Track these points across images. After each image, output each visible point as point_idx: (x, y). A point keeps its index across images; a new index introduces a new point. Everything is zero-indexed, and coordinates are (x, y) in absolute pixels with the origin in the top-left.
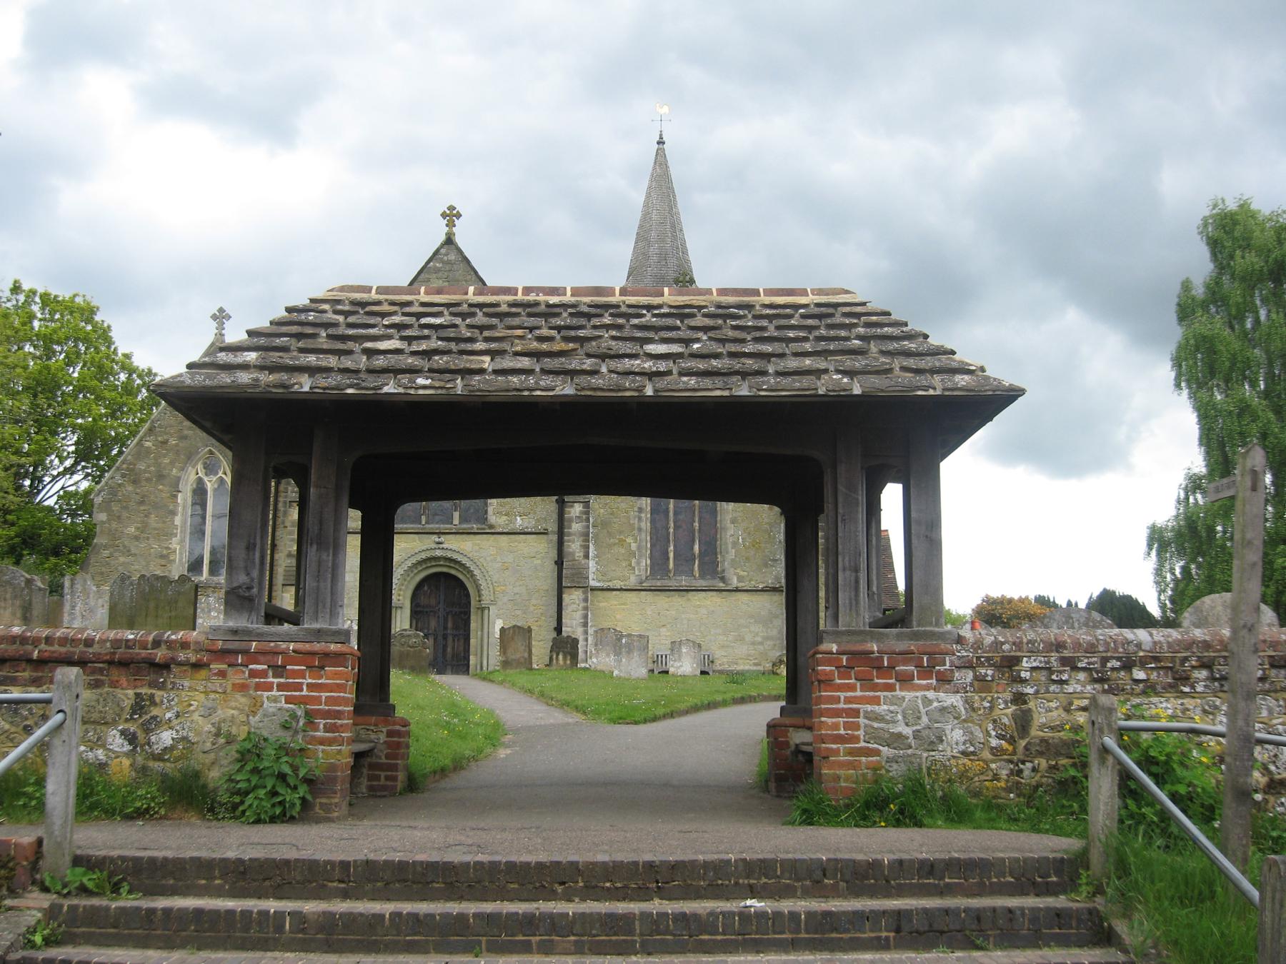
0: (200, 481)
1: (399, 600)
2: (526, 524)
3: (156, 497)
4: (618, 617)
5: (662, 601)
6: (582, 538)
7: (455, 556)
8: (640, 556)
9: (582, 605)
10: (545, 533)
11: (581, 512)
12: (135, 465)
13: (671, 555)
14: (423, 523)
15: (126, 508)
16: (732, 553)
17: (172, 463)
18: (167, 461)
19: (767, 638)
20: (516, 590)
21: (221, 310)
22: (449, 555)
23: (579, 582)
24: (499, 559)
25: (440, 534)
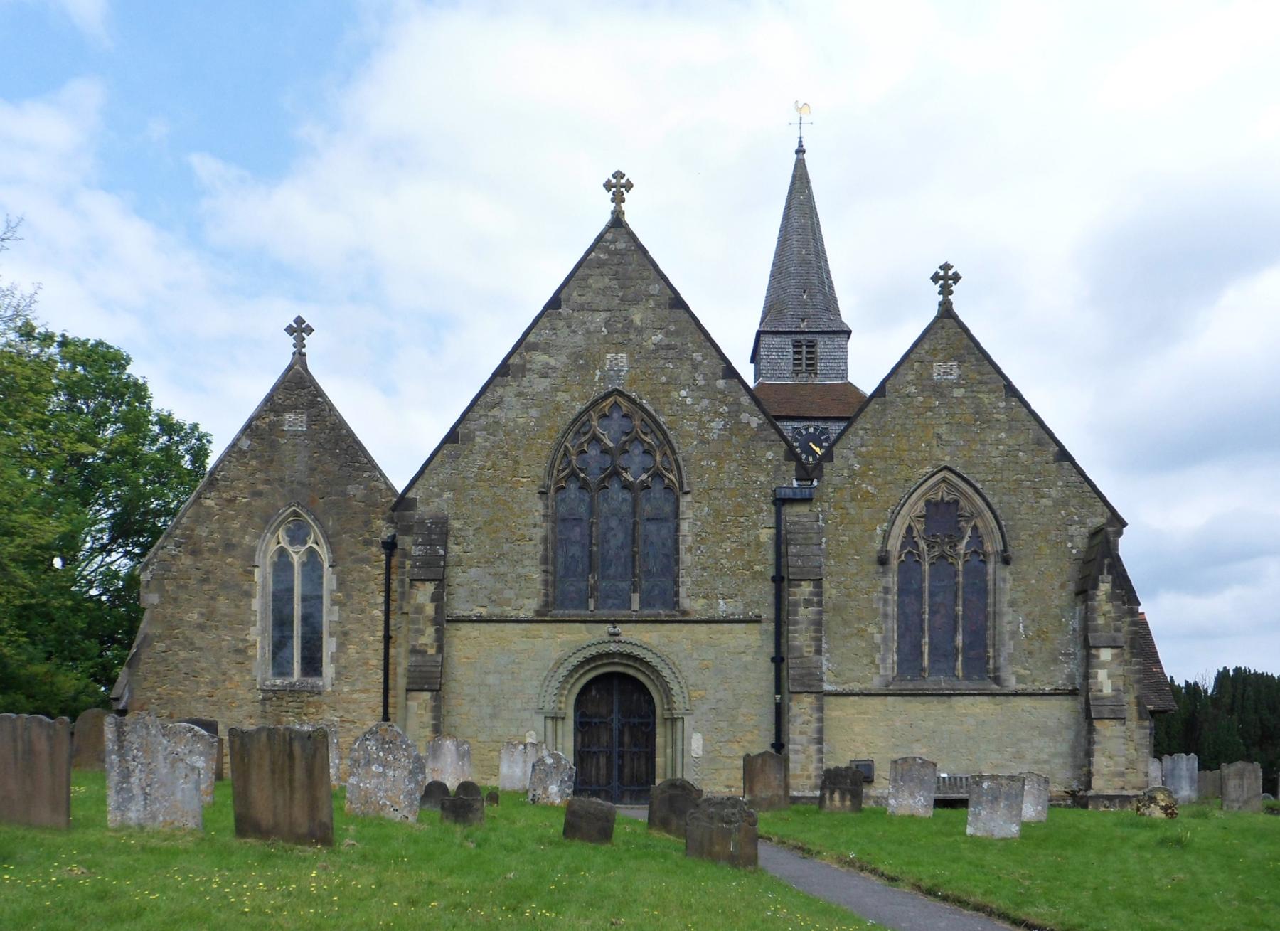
0: (282, 552)
1: (560, 709)
2: (731, 610)
3: (225, 573)
4: (857, 729)
5: (915, 707)
6: (812, 628)
7: (636, 651)
9: (816, 716)
10: (757, 620)
11: (811, 594)
12: (193, 530)
13: (926, 649)
14: (592, 608)
15: (185, 587)
16: (1009, 647)
17: (244, 529)
19: (1054, 755)
20: (719, 696)
22: (628, 649)
23: (810, 686)
24: (695, 656)
25: (614, 622)
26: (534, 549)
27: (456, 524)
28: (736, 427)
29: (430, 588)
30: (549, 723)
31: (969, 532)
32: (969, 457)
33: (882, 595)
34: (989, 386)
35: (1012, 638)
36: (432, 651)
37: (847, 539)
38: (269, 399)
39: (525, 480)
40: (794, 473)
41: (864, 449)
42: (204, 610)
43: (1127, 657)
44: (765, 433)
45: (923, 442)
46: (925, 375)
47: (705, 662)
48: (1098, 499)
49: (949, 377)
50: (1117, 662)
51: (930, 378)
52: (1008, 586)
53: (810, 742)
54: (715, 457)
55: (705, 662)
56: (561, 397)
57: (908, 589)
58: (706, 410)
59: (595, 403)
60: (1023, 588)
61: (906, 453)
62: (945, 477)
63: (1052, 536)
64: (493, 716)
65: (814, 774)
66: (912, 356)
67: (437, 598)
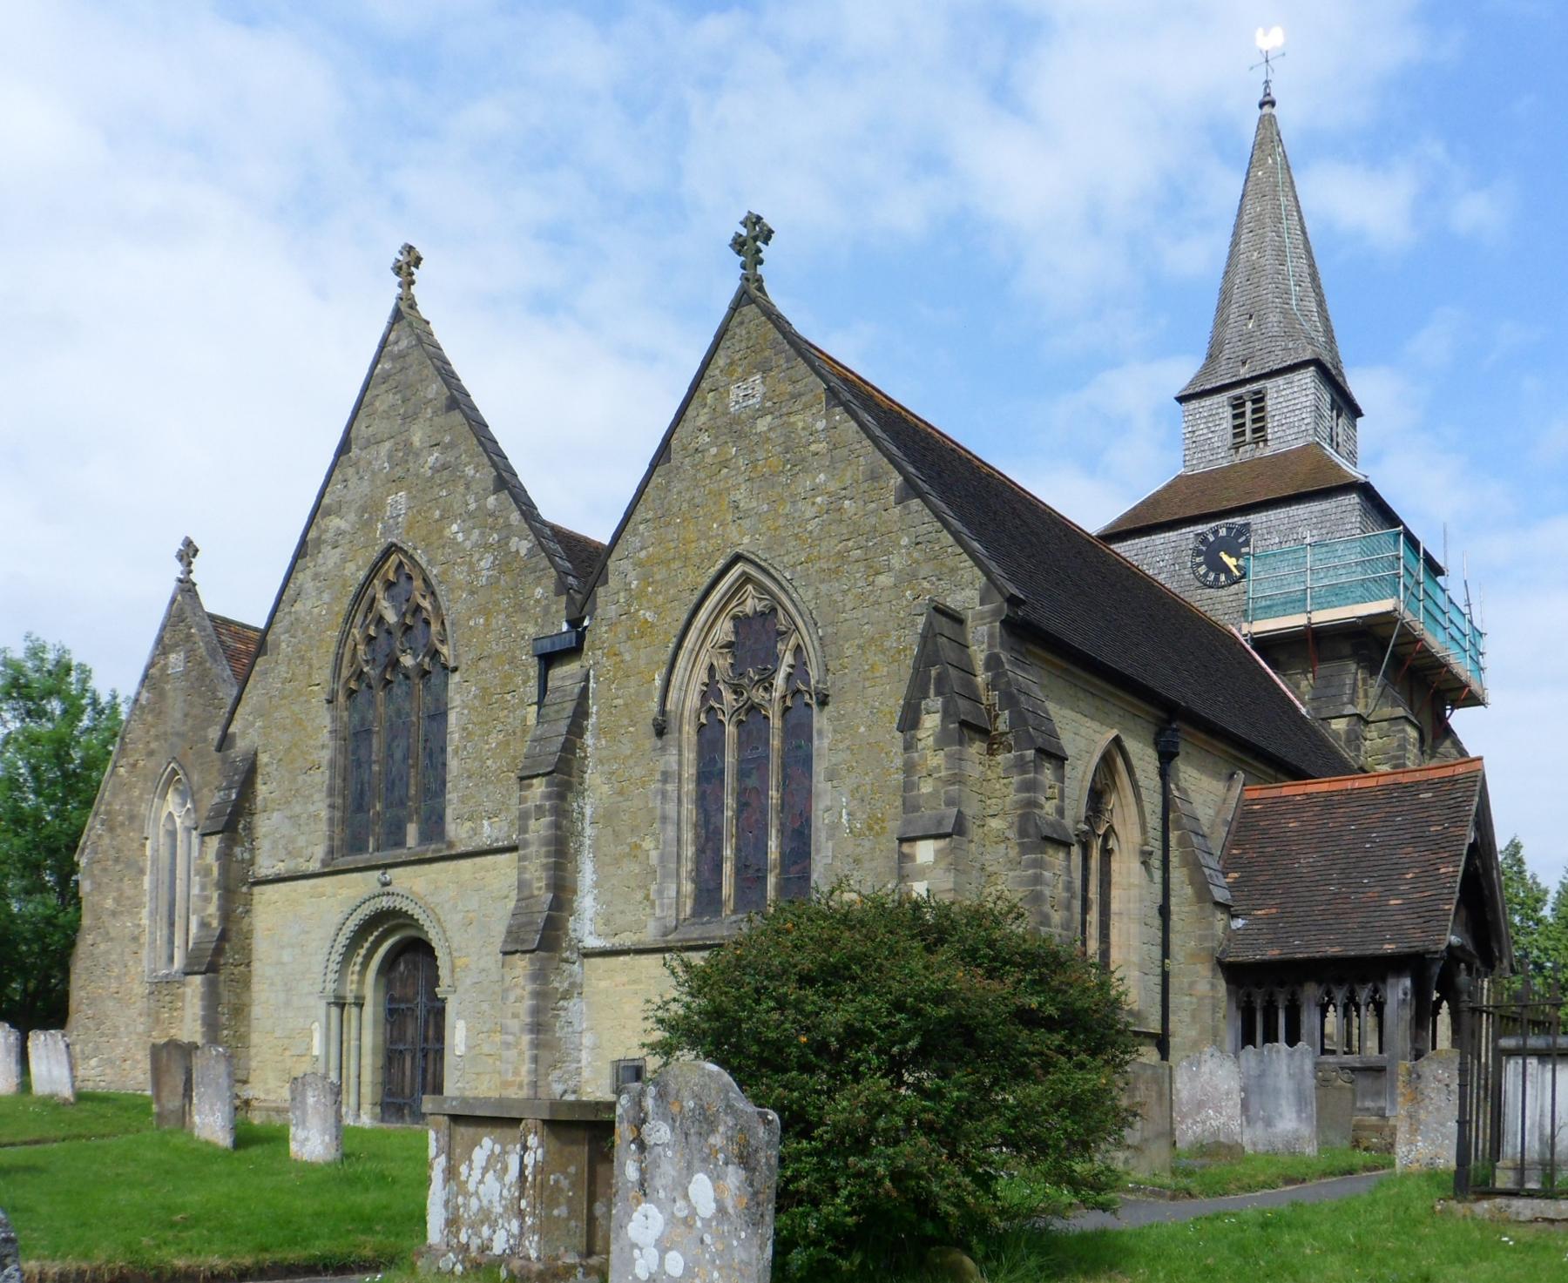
2: (495, 834)
8: (664, 876)
18: (136, 793)
21: (188, 543)
23: (524, 942)
26: (321, 777)
27: (263, 758)
28: (506, 562)
29: (214, 843)
30: (335, 1011)
31: (788, 658)
32: (776, 529)
33: (659, 785)
34: (804, 399)
35: (830, 837)
36: (215, 923)
37: (620, 702)
38: (160, 640)
39: (316, 688)
40: (564, 613)
41: (643, 554)
42: (115, 894)
43: (1014, 852)
44: (534, 560)
45: (715, 520)
46: (719, 409)
47: (471, 915)
48: (965, 556)
49: (750, 402)
50: (943, 865)
51: (726, 413)
52: (826, 742)
53: (522, 1031)
54: (485, 611)
55: (471, 915)
56: (351, 567)
57: (709, 774)
58: (476, 545)
59: (375, 569)
60: (847, 742)
61: (693, 545)
62: (744, 573)
63: (890, 643)
64: (288, 1003)
65: (526, 1080)
66: (704, 385)
67: (225, 855)
